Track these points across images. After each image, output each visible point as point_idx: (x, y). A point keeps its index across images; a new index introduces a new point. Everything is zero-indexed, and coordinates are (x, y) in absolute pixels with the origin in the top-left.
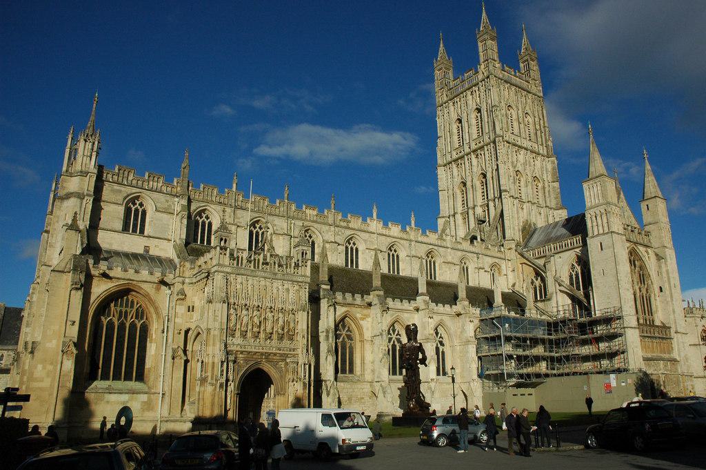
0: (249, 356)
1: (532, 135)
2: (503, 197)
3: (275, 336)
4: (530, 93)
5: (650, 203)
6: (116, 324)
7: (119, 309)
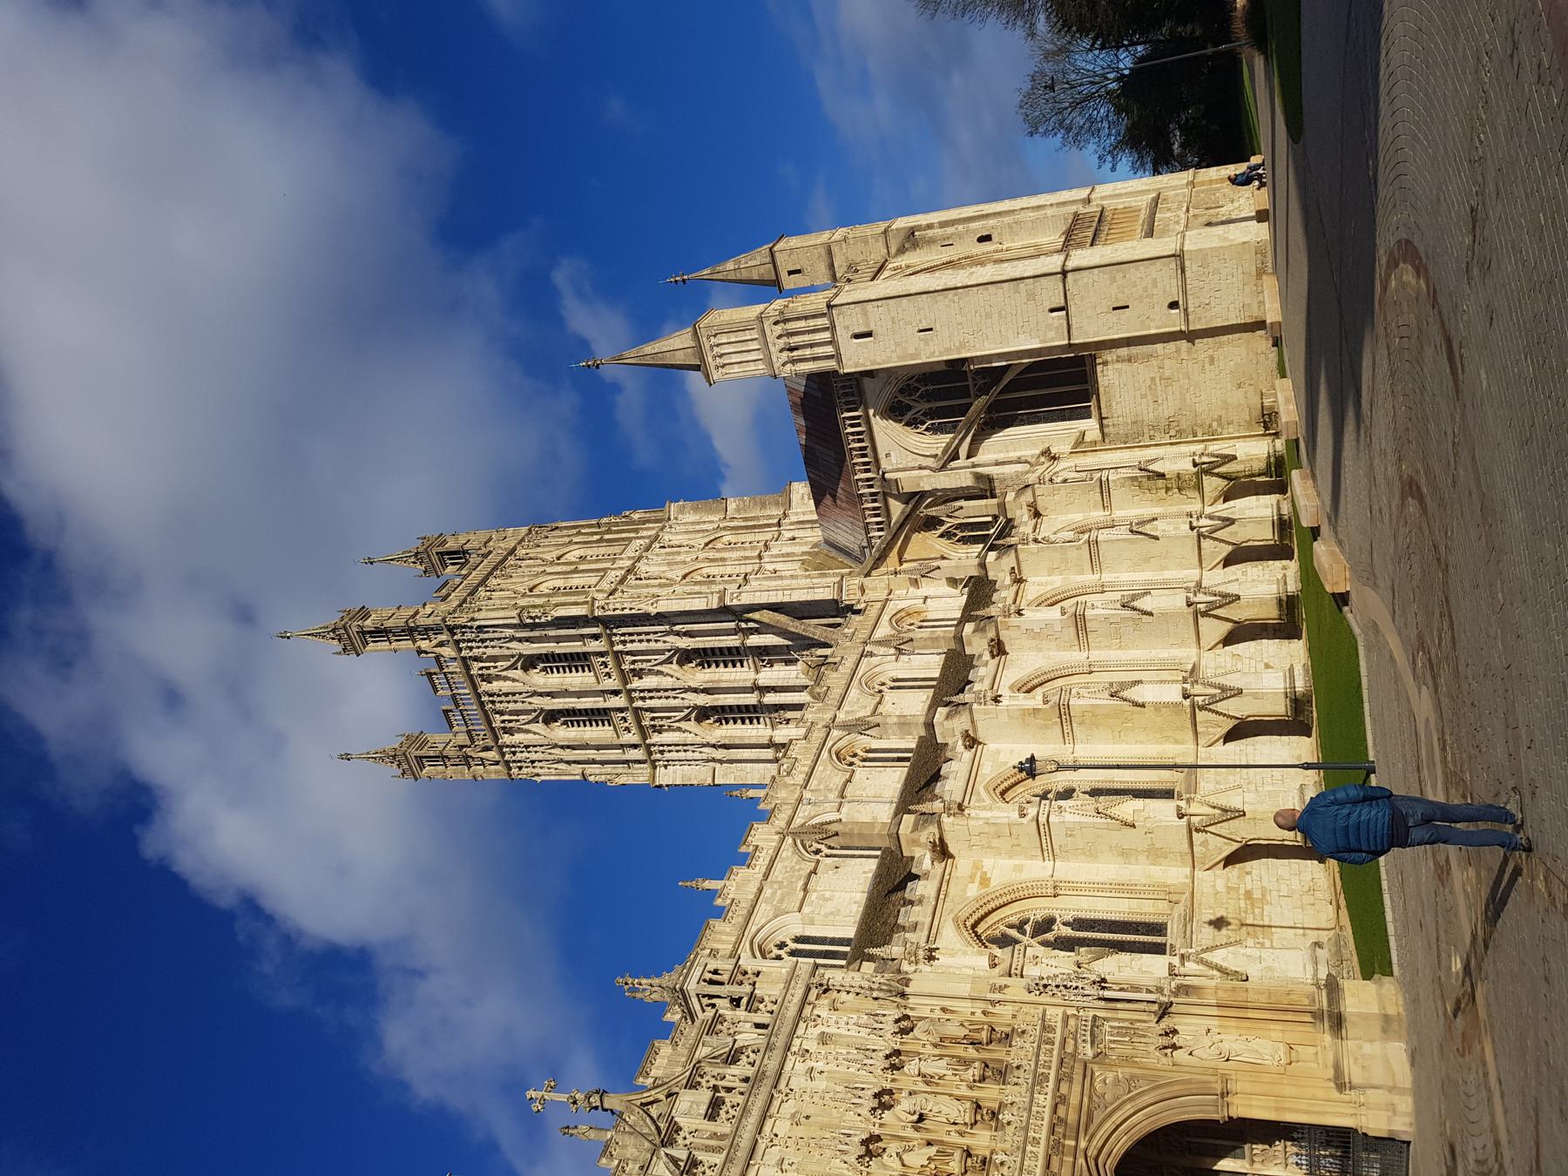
1: (610, 550)
2: (735, 602)
3: (990, 1094)
4: (514, 549)
5: (784, 264)
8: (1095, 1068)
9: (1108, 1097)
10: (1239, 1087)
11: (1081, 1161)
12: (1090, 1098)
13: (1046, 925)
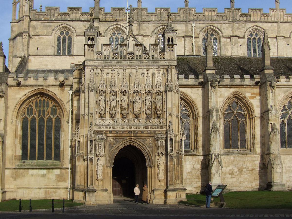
0: (118, 135)
6: (38, 119)
7: (38, 109)
8: (153, 139)
9: (146, 142)
10: (153, 170)
11: (128, 138)
12: (145, 138)
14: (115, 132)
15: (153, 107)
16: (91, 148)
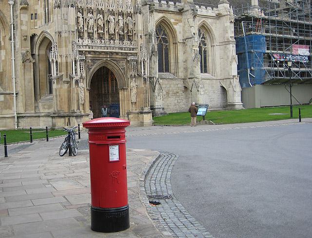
0: (96, 56)
13: (166, 42)
14: (93, 53)
15: (125, 29)
16: (76, 70)
